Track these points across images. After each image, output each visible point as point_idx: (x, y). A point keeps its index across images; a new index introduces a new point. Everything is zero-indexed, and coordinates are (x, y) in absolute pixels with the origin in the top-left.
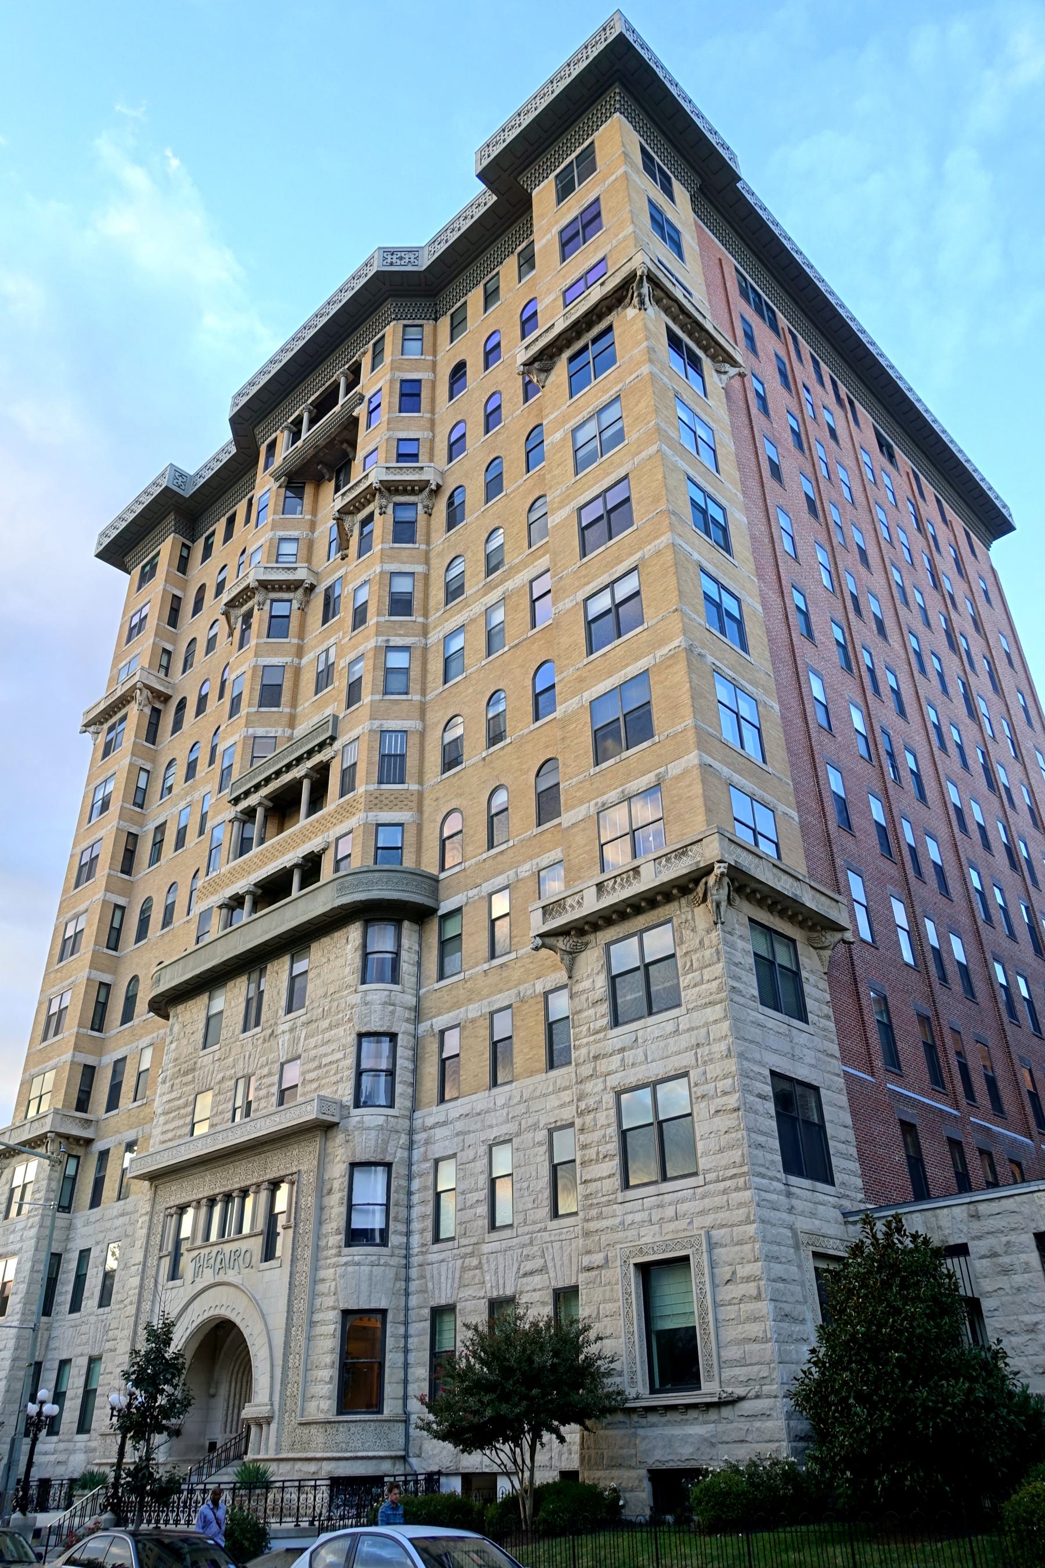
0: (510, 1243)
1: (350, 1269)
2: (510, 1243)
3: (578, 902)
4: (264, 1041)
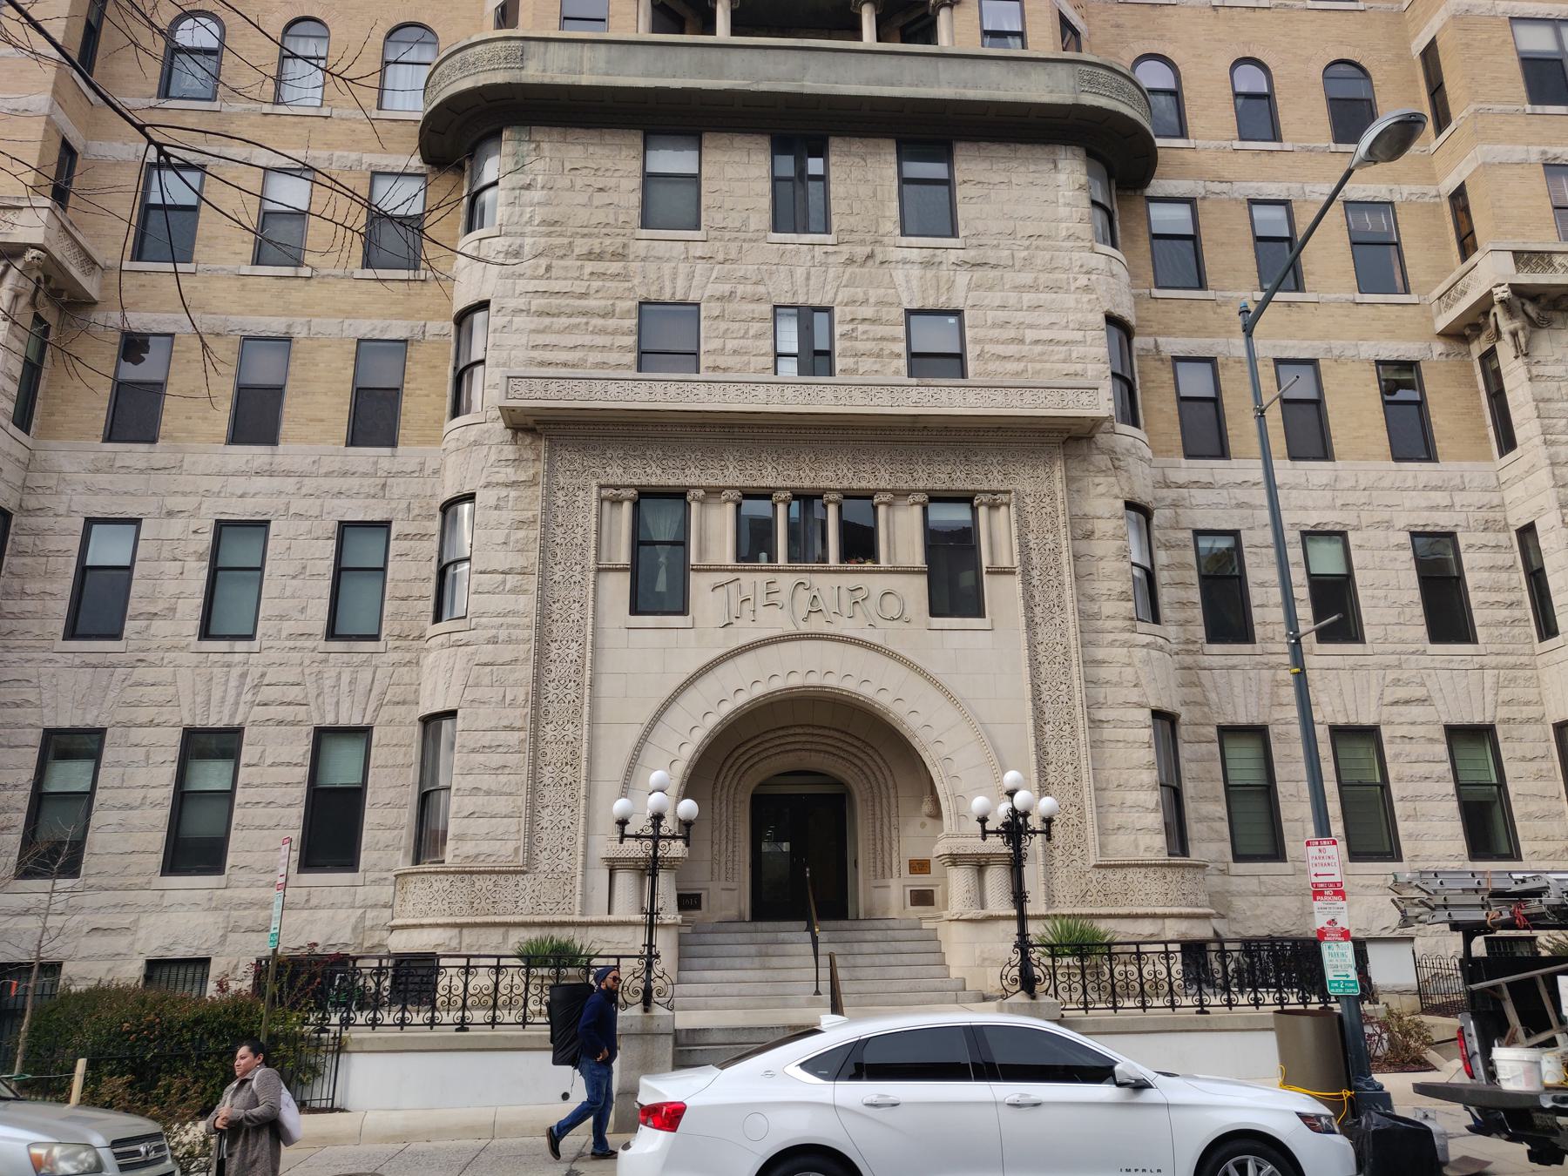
0: (1362, 661)
1: (1154, 653)
2: (1362, 661)
4: (851, 261)
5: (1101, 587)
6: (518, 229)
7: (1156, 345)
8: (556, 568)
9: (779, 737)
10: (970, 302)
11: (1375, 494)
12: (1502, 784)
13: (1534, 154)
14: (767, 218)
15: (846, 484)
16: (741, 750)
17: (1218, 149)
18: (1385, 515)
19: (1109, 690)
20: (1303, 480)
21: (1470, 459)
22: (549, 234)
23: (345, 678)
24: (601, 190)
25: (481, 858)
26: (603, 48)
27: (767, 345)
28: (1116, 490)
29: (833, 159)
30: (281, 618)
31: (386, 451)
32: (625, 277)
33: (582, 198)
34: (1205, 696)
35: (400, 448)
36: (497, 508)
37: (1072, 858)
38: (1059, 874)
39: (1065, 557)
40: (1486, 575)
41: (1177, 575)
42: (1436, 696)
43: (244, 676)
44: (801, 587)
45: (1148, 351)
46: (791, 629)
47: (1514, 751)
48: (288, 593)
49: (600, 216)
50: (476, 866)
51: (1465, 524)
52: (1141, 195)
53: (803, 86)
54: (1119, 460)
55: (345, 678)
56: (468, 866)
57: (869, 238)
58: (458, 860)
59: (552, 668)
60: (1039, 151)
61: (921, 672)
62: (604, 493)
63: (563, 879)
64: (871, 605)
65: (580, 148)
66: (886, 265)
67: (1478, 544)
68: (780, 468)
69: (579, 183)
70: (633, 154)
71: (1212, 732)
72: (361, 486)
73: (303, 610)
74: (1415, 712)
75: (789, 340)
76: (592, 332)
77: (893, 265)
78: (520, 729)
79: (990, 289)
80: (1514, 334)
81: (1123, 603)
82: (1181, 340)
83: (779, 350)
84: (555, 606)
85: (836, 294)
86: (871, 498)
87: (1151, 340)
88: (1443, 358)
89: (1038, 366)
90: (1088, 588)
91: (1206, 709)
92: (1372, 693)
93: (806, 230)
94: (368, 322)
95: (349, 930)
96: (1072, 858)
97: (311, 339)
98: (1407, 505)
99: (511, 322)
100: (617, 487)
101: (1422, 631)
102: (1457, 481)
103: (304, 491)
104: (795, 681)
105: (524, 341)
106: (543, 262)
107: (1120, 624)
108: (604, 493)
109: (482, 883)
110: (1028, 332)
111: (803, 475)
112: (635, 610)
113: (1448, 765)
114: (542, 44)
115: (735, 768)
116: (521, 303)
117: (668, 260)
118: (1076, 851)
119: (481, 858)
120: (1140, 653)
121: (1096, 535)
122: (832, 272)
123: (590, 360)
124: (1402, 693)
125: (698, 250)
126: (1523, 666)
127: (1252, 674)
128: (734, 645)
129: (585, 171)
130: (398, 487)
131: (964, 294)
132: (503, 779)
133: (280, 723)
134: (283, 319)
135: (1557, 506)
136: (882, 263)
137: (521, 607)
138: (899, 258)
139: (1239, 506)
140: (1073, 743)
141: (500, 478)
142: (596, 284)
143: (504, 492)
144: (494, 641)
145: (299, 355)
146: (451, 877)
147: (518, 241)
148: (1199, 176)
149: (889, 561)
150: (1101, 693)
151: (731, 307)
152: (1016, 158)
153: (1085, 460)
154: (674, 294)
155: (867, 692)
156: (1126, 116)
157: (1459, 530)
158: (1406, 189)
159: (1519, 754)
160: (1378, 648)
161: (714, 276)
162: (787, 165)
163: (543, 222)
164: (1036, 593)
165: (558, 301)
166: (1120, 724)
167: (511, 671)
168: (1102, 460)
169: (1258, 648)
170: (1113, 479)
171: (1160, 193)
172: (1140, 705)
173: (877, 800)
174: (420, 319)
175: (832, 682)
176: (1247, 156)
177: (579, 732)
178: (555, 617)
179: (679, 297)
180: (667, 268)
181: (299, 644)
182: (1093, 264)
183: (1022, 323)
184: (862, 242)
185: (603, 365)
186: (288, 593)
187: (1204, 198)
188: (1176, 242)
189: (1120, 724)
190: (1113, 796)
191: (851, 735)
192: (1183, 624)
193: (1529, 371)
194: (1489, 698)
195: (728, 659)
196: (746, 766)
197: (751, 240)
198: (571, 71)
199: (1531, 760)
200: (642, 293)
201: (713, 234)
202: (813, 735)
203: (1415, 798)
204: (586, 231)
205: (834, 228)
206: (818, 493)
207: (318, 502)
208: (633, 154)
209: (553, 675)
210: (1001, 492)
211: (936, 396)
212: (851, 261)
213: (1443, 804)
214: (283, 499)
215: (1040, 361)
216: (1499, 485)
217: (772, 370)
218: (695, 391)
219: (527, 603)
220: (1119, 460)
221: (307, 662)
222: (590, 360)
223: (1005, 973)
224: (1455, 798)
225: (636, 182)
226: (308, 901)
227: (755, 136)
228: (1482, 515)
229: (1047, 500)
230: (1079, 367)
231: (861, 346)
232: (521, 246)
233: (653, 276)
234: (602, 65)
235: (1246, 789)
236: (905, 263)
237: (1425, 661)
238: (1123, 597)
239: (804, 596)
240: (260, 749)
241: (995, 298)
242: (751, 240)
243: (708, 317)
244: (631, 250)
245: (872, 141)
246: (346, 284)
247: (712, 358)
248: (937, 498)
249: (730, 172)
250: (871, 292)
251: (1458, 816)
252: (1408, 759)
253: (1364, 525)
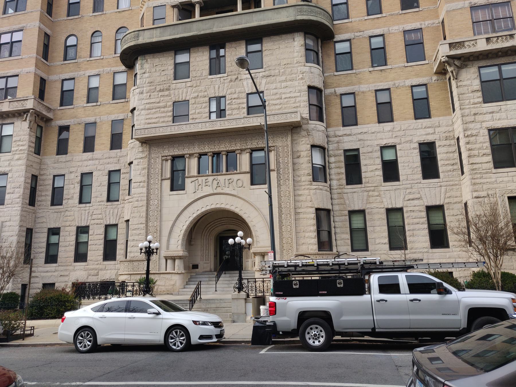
0: (398, 187)
1: (318, 191)
2: (398, 187)
3: (473, 44)
4: (231, 81)
5: (302, 172)
6: (142, 86)
7: (335, 91)
8: (152, 180)
9: (219, 221)
10: (266, 88)
11: (407, 131)
12: (445, 224)
13: (467, 4)
14: (208, 71)
15: (227, 149)
17: (359, 20)
18: (410, 138)
19: (302, 203)
20: (382, 129)
21: (443, 115)
22: (150, 86)
23: (111, 212)
24: (163, 71)
25: (135, 257)
26: (159, 29)
27: (207, 110)
28: (308, 142)
29: (227, 50)
30: (96, 197)
31: (119, 150)
32: (169, 95)
33: (158, 74)
34: (345, 202)
35: (122, 149)
36: (138, 165)
37: (289, 253)
38: (285, 257)
39: (290, 165)
40: (445, 155)
41: (337, 165)
42: (423, 196)
43: (89, 213)
44: (215, 180)
45: (332, 93)
46: (212, 192)
47: (450, 213)
48: (98, 191)
49: (163, 79)
50: (134, 259)
51: (439, 139)
52: (333, 41)
53: (213, 30)
54: (309, 132)
55: (111, 212)
56: (132, 259)
57: (237, 73)
58: (130, 258)
59: (151, 207)
60: (289, 36)
61: (247, 202)
62: (163, 158)
63: (154, 262)
64: (234, 183)
65: (158, 59)
66: (241, 80)
67: (443, 145)
68: (210, 146)
69: (158, 69)
70: (171, 58)
71: (346, 213)
72: (113, 160)
73: (101, 195)
74: (416, 202)
75: (214, 108)
76: (161, 113)
77: (243, 80)
78: (144, 224)
79: (272, 83)
80: (452, 72)
81: (309, 177)
82: (343, 88)
83: (211, 111)
84: (151, 190)
85: (227, 92)
86: (235, 152)
87: (333, 90)
88: (436, 81)
89: (286, 106)
90: (297, 173)
91: (345, 206)
92: (401, 197)
93: (220, 73)
94: (114, 115)
95: (114, 275)
96: (289, 253)
97: (101, 122)
98: (418, 134)
99: (140, 113)
100: (166, 156)
101: (420, 176)
102: (437, 124)
103: (100, 163)
104: (213, 207)
105: (144, 118)
106: (149, 94)
107: (307, 183)
108: (163, 158)
109: (136, 264)
110: (283, 95)
111: (216, 147)
112: (172, 189)
113: (426, 219)
114: (143, 31)
115: (208, 230)
116: (142, 107)
117: (181, 89)
118: (290, 250)
119: (135, 257)
120: (312, 192)
121: (301, 157)
122: (226, 85)
123: (161, 121)
124: (411, 197)
125: (189, 84)
126: (456, 185)
127: (360, 194)
128: (196, 198)
129: (159, 66)
130: (122, 160)
131: (264, 86)
132: (140, 237)
133: (97, 224)
134: (94, 117)
135: (463, 130)
136: (240, 80)
137: (144, 191)
138: (245, 78)
139: (359, 140)
140: (290, 219)
141: (139, 157)
142: (162, 99)
143: (139, 160)
144: (138, 201)
145: (98, 127)
146: (128, 262)
147: (142, 89)
148: (353, 31)
149: (240, 170)
150: (299, 204)
151: (197, 100)
152: (282, 39)
153: (298, 134)
154: (182, 98)
155: (233, 209)
156: (313, 20)
157: (436, 141)
158: (427, 23)
159: (452, 214)
160: (404, 182)
161: (193, 91)
162: (214, 53)
163: (148, 83)
164: (281, 176)
165: (152, 105)
166: (305, 213)
167: (142, 209)
168: (304, 133)
169: (363, 185)
170: (307, 139)
171: (339, 39)
172: (312, 207)
174: (127, 113)
175: (223, 206)
176: (370, 21)
177: (158, 224)
178: (151, 193)
179: (184, 99)
180: (180, 91)
181: (101, 204)
182: (304, 70)
183: (281, 93)
184: (235, 74)
185: (163, 122)
186: (98, 191)
187: (354, 39)
188: (345, 55)
189: (305, 213)
190: (302, 234)
191: (238, 220)
192: (339, 180)
193: (457, 84)
194: (443, 196)
195: (195, 202)
196: (211, 229)
197: (203, 79)
198: (151, 38)
199: (456, 216)
200: (174, 100)
201: (193, 79)
203: (413, 230)
204: (159, 83)
205: (227, 71)
206: (220, 152)
207: (104, 166)
208: (171, 58)
209: (151, 209)
210: (272, 147)
211: (249, 121)
212: (231, 81)
213: (423, 231)
214: (96, 166)
215: (286, 104)
216: (453, 123)
217: (208, 118)
218: (182, 127)
219: (145, 190)
220: (309, 132)
221: (103, 208)
222: (161, 121)
223: (235, 286)
224: (427, 229)
225: (172, 67)
226: (105, 268)
227: (205, 47)
228: (444, 135)
229: (286, 147)
230: (298, 104)
231: (233, 107)
232: (143, 91)
233: (177, 94)
234: (158, 34)
235: (358, 229)
236: (247, 79)
237: (421, 185)
238: (308, 175)
239: (215, 182)
240: (93, 231)
241: (273, 86)
242: (203, 79)
243: (191, 104)
244: (171, 87)
245: (238, 42)
246: (108, 105)
247: (192, 116)
248: (253, 150)
249: (198, 59)
250: (237, 89)
251: (428, 235)
252: (412, 218)
253: (402, 142)
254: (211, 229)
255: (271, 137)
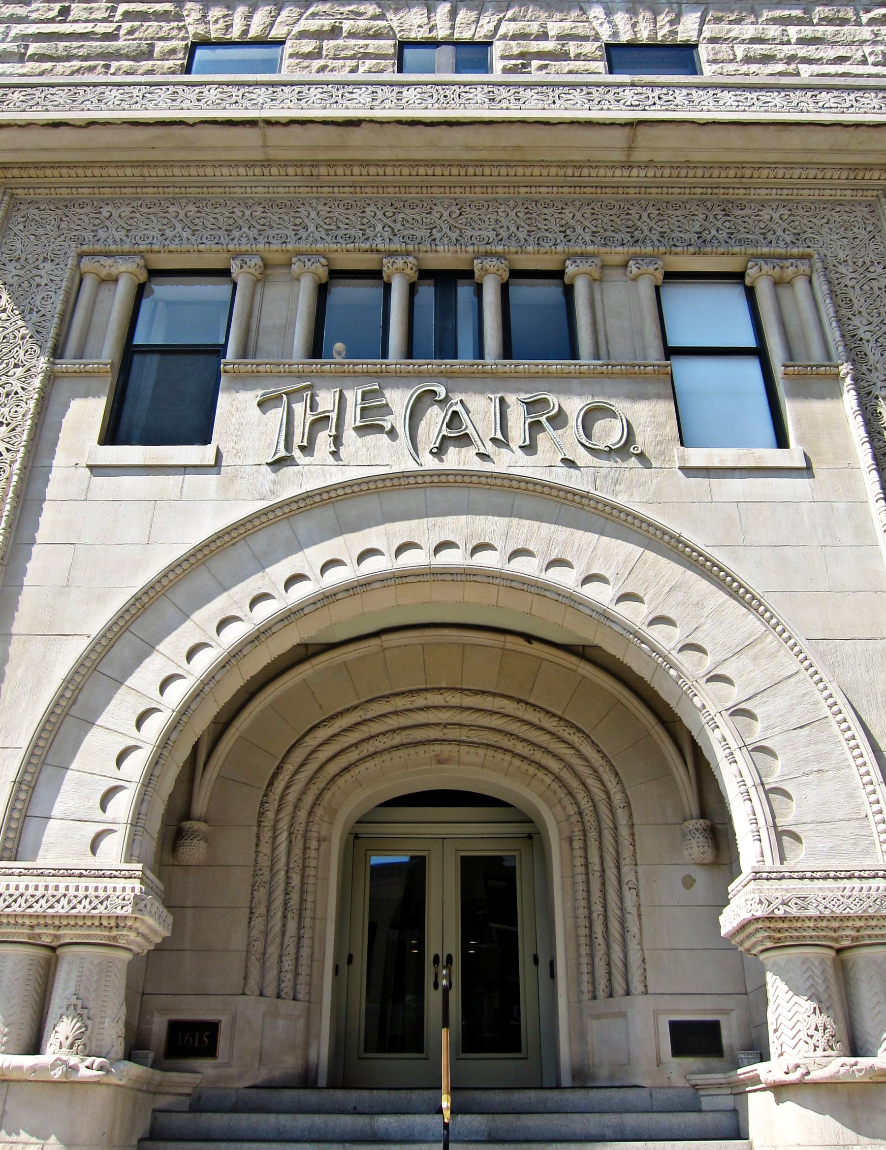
9: (396, 713)
16: (322, 734)
108: (87, 264)
173: (592, 835)
196: (333, 768)
202: (462, 709)
250: (550, 25)
254: (333, 768)
255: (776, 216)
